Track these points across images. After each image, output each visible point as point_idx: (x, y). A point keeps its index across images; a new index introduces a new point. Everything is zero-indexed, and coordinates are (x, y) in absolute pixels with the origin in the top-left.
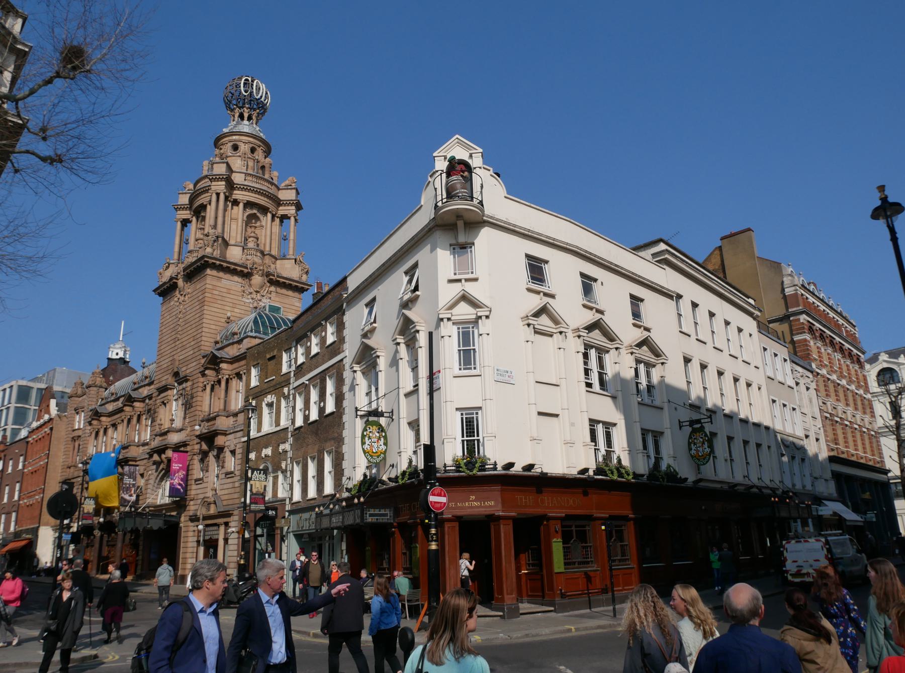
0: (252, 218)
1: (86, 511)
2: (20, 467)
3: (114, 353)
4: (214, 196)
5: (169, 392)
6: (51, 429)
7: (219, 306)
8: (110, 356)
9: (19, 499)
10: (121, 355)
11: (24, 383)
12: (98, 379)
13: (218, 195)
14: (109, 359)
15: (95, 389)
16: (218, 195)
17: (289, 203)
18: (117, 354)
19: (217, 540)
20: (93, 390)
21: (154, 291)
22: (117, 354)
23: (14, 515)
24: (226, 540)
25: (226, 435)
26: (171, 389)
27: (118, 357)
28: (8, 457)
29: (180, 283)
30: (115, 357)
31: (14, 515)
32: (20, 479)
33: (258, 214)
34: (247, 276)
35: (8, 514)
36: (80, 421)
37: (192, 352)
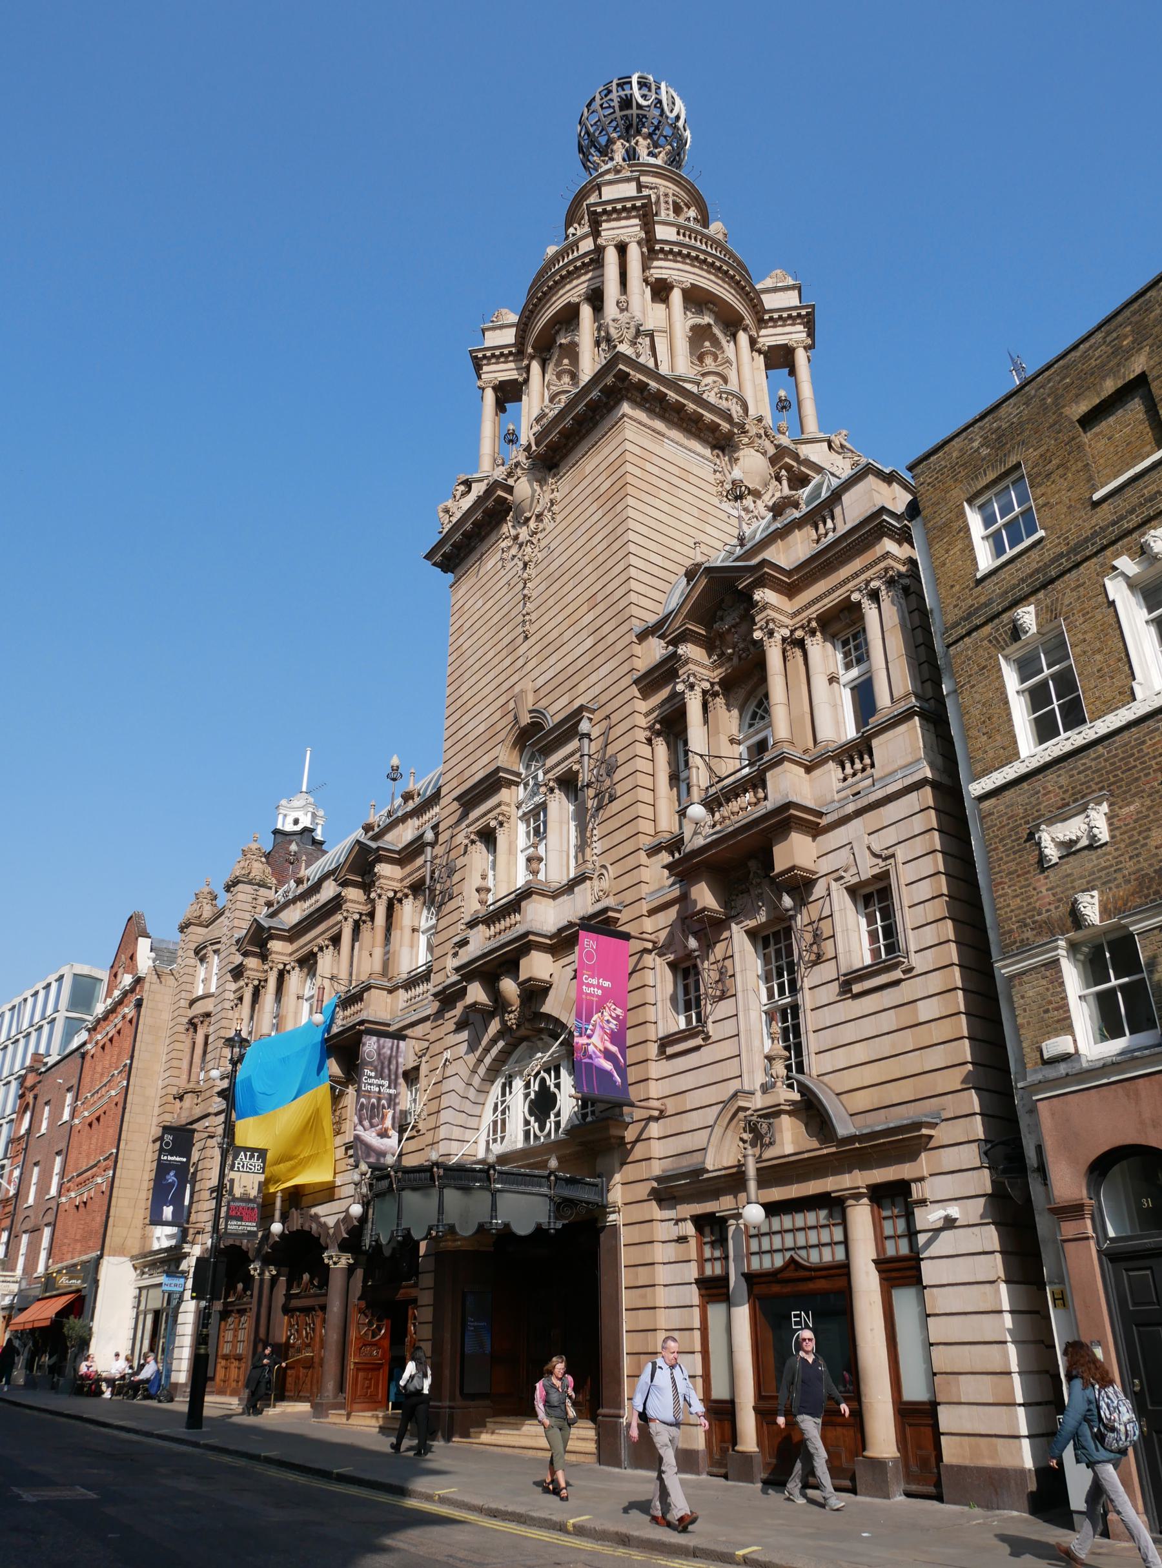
0: (699, 335)
1: (238, 1192)
2: (66, 1116)
3: (290, 820)
4: (611, 256)
5: (504, 794)
6: (139, 1004)
7: (666, 508)
8: (279, 826)
9: (60, 1194)
10: (306, 821)
11: (84, 969)
12: (256, 865)
13: (622, 249)
14: (276, 832)
15: (248, 888)
16: (622, 249)
17: (785, 318)
18: (296, 822)
19: (843, 1271)
20: (244, 892)
21: (428, 557)
22: (296, 822)
23: (47, 1231)
24: (901, 1272)
25: (816, 831)
26: (510, 784)
27: (298, 828)
28: (41, 1101)
29: (523, 487)
30: (289, 827)
31: (47, 1231)
32: (62, 1145)
33: (716, 331)
34: (723, 443)
35: (35, 1230)
36: (208, 978)
37: (589, 643)
